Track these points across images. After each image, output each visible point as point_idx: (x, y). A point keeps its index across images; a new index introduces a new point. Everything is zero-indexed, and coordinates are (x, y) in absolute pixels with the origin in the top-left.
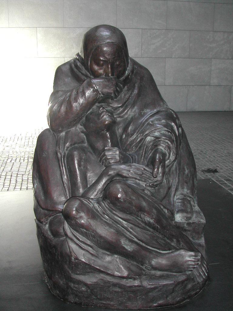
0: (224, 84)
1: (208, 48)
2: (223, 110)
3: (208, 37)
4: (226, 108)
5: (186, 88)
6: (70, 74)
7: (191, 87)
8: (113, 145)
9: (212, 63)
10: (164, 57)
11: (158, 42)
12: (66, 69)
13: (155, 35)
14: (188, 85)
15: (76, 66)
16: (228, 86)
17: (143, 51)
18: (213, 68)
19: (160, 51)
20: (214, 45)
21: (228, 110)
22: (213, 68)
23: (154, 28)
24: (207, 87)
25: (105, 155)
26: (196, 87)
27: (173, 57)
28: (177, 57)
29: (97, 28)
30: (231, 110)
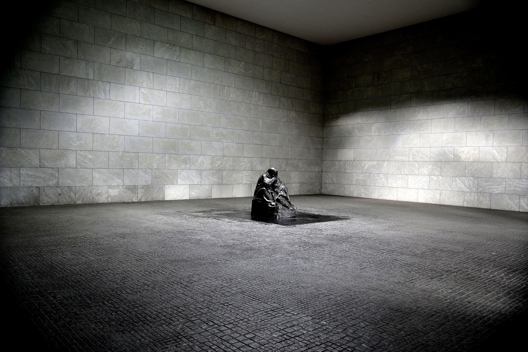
3: (241, 160)
15: (268, 175)
18: (243, 175)
19: (220, 167)
20: (243, 164)
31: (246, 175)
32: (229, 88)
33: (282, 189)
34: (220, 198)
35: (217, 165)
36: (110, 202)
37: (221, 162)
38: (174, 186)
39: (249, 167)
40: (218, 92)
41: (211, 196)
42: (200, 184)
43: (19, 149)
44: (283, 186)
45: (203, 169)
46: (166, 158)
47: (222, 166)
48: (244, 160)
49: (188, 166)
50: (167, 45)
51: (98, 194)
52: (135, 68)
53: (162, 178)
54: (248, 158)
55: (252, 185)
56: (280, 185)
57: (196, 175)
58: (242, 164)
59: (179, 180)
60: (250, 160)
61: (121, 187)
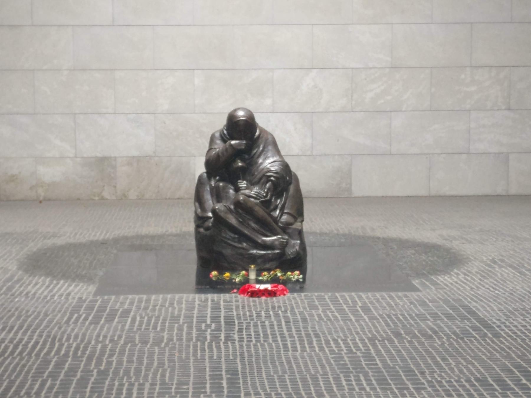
2: (496, 194)
3: (463, 76)
4: (500, 190)
5: (427, 158)
6: (220, 138)
8: (243, 180)
10: (388, 110)
12: (217, 135)
14: (430, 154)
15: (224, 134)
16: (502, 153)
17: (354, 103)
18: (473, 125)
19: (382, 101)
20: (473, 88)
21: (504, 193)
22: (473, 125)
23: (371, 66)
24: (464, 156)
25: (238, 185)
27: (404, 109)
33: (261, 179)
34: (384, 198)
37: (382, 88)
42: (309, 153)
44: (272, 169)
45: (321, 110)
46: (197, 81)
47: (389, 98)
49: (268, 102)
56: (262, 163)
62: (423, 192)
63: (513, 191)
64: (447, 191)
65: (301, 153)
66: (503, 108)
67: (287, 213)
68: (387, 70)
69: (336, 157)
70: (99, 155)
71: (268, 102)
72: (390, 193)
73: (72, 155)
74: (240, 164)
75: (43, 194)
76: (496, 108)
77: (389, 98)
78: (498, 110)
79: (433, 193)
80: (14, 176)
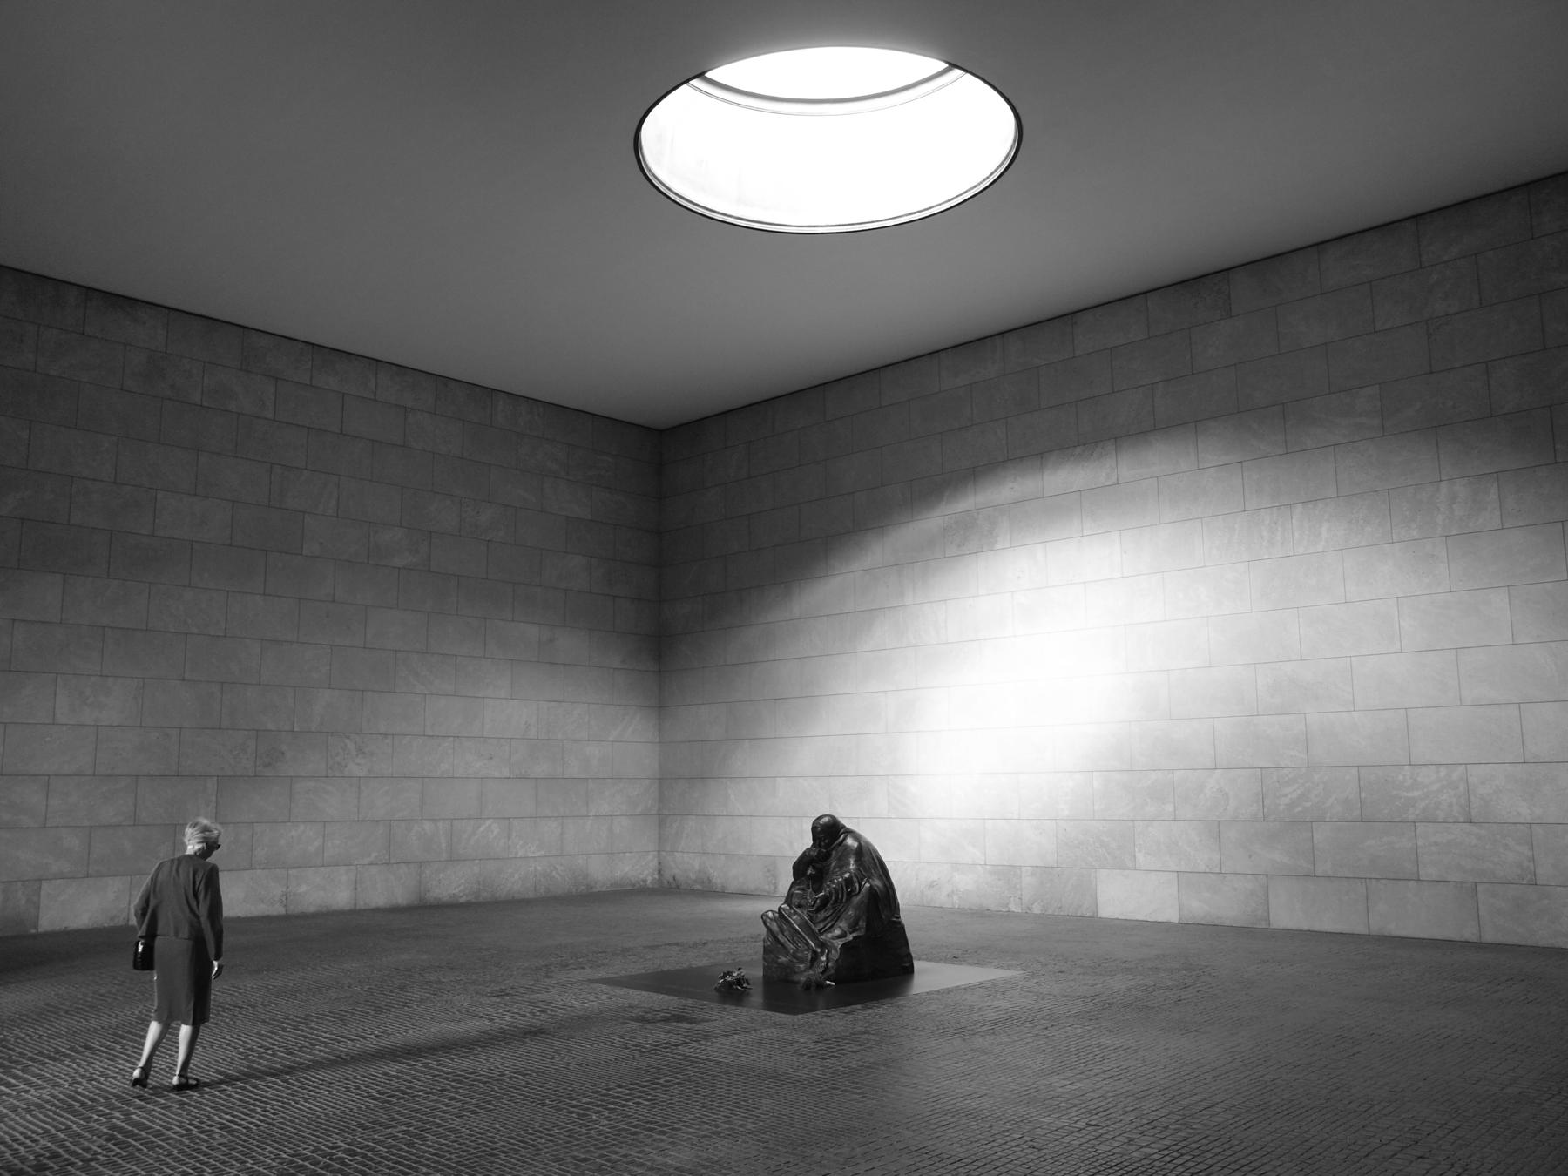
0: (1454, 879)
1: (1403, 800)
2: (1463, 939)
4: (1469, 934)
7: (1374, 882)
9: (1418, 831)
11: (1295, 791)
13: (1287, 778)
17: (1265, 810)
19: (1300, 809)
21: (1474, 939)
23: (1283, 766)
26: (1383, 881)
27: (1327, 819)
28: (1334, 820)
29: (819, 818)
30: (1483, 940)
31: (1436, 844)
32: (1310, 506)
35: (1286, 800)
36: (957, 906)
37: (1299, 792)
38: (1126, 872)
39: (1451, 805)
40: (1265, 534)
41: (1268, 920)
42: (1217, 870)
43: (801, 780)
47: (1309, 804)
48: (1419, 779)
50: (1078, 450)
51: (931, 885)
52: (998, 546)
53: (1087, 848)
54: (1443, 772)
55: (1480, 888)
57: (1201, 841)
58: (1410, 795)
59: (1140, 856)
60: (1455, 776)
61: (980, 868)
62: (1361, 929)
63: (1489, 937)
64: (1394, 929)
65: (1208, 870)
66: (1462, 819)
67: (840, 927)
68: (1304, 770)
69: (1249, 876)
70: (1006, 864)
71: (1170, 808)
72: (1317, 927)
73: (983, 863)
74: (809, 872)
75: (957, 902)
76: (1451, 820)
77: (1309, 804)
78: (1454, 822)
79: (1375, 930)
80: (934, 881)
